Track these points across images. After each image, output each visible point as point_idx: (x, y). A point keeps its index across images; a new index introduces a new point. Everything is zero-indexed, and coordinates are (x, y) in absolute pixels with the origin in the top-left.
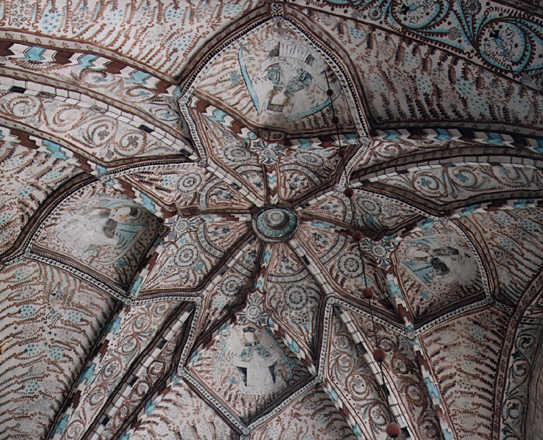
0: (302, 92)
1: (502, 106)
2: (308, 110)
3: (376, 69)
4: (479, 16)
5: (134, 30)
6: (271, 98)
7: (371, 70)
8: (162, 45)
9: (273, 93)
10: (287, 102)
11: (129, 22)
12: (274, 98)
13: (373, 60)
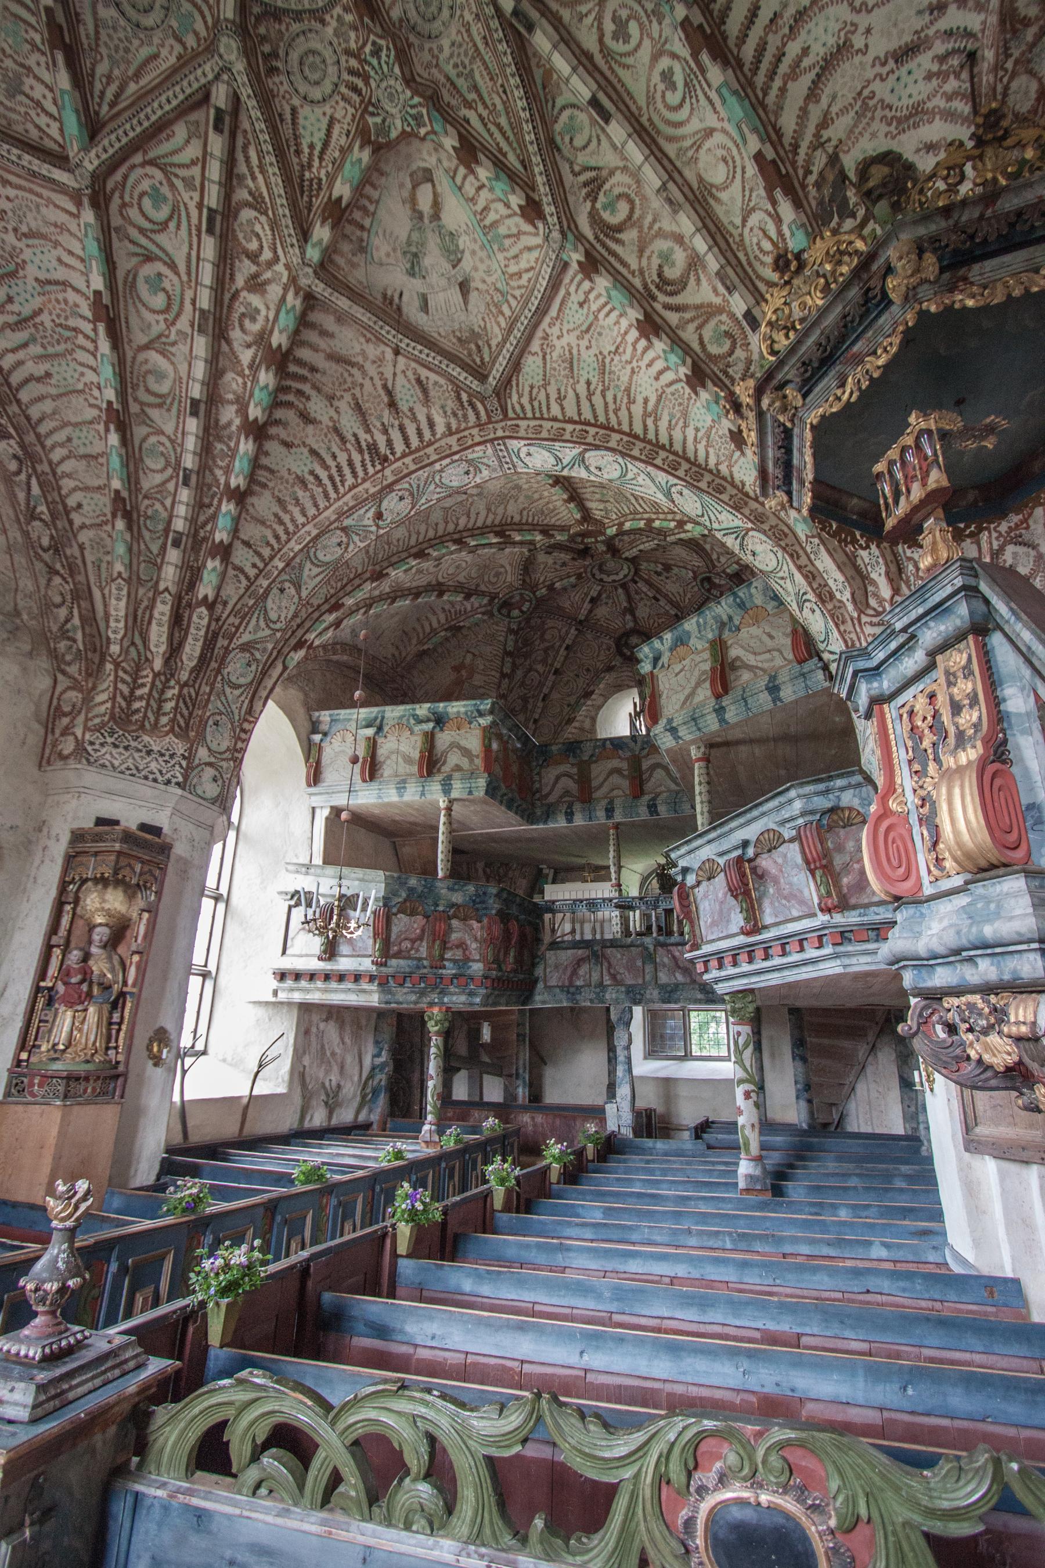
0: (403, 236)
1: (271, 484)
2: (382, 213)
3: (360, 359)
4: (356, 538)
5: (627, 356)
6: (435, 195)
7: (363, 353)
8: (596, 318)
9: (436, 205)
10: (413, 200)
11: (633, 371)
12: (431, 196)
13: (372, 370)
